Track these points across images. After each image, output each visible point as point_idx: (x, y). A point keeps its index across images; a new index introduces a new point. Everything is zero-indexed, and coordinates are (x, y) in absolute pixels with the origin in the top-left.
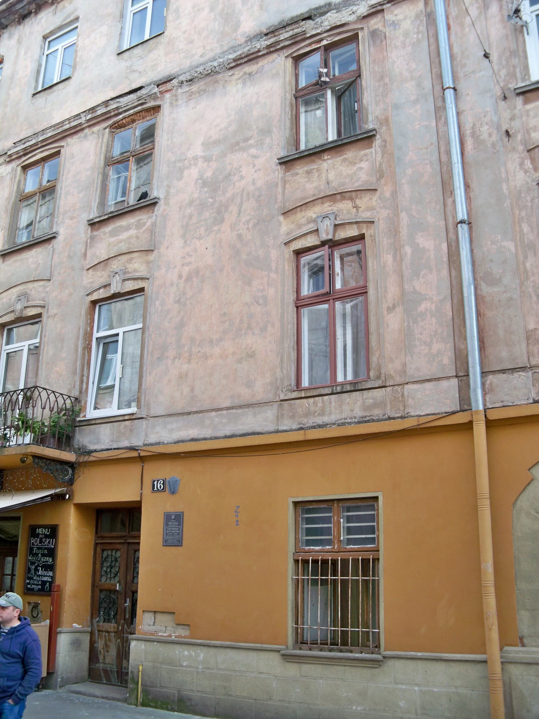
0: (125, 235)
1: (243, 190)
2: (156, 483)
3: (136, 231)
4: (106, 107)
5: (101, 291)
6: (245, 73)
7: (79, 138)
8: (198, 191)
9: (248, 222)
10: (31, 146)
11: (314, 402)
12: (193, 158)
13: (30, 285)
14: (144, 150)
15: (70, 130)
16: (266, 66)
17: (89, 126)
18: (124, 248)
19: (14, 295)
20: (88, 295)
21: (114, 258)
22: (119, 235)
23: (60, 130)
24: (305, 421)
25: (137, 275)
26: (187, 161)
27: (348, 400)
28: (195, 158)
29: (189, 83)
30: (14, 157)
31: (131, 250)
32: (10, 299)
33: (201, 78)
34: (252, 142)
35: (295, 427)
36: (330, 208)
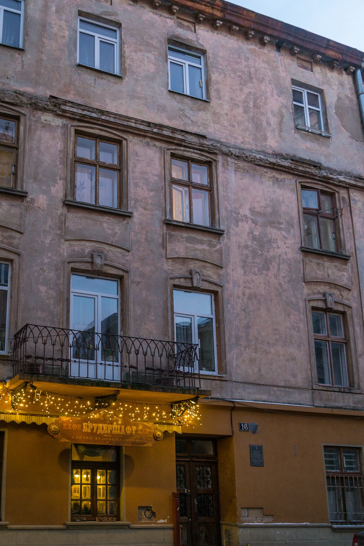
0: (199, 247)
1: (280, 255)
2: (242, 425)
3: (208, 248)
5: (182, 280)
6: (274, 177)
7: (140, 141)
8: (251, 242)
9: (284, 277)
11: (331, 394)
12: (244, 215)
13: (107, 248)
14: (202, 188)
15: (134, 130)
16: (286, 180)
17: (151, 138)
18: (200, 255)
19: (88, 248)
20: (171, 279)
21: (190, 260)
22: (195, 244)
23: (126, 123)
24: (327, 403)
25: (211, 280)
26: (240, 215)
27: (346, 397)
28: (245, 216)
29: (236, 158)
30: (68, 115)
31: (206, 260)
32: (83, 250)
33: (245, 160)
35: (322, 405)
36: (329, 290)
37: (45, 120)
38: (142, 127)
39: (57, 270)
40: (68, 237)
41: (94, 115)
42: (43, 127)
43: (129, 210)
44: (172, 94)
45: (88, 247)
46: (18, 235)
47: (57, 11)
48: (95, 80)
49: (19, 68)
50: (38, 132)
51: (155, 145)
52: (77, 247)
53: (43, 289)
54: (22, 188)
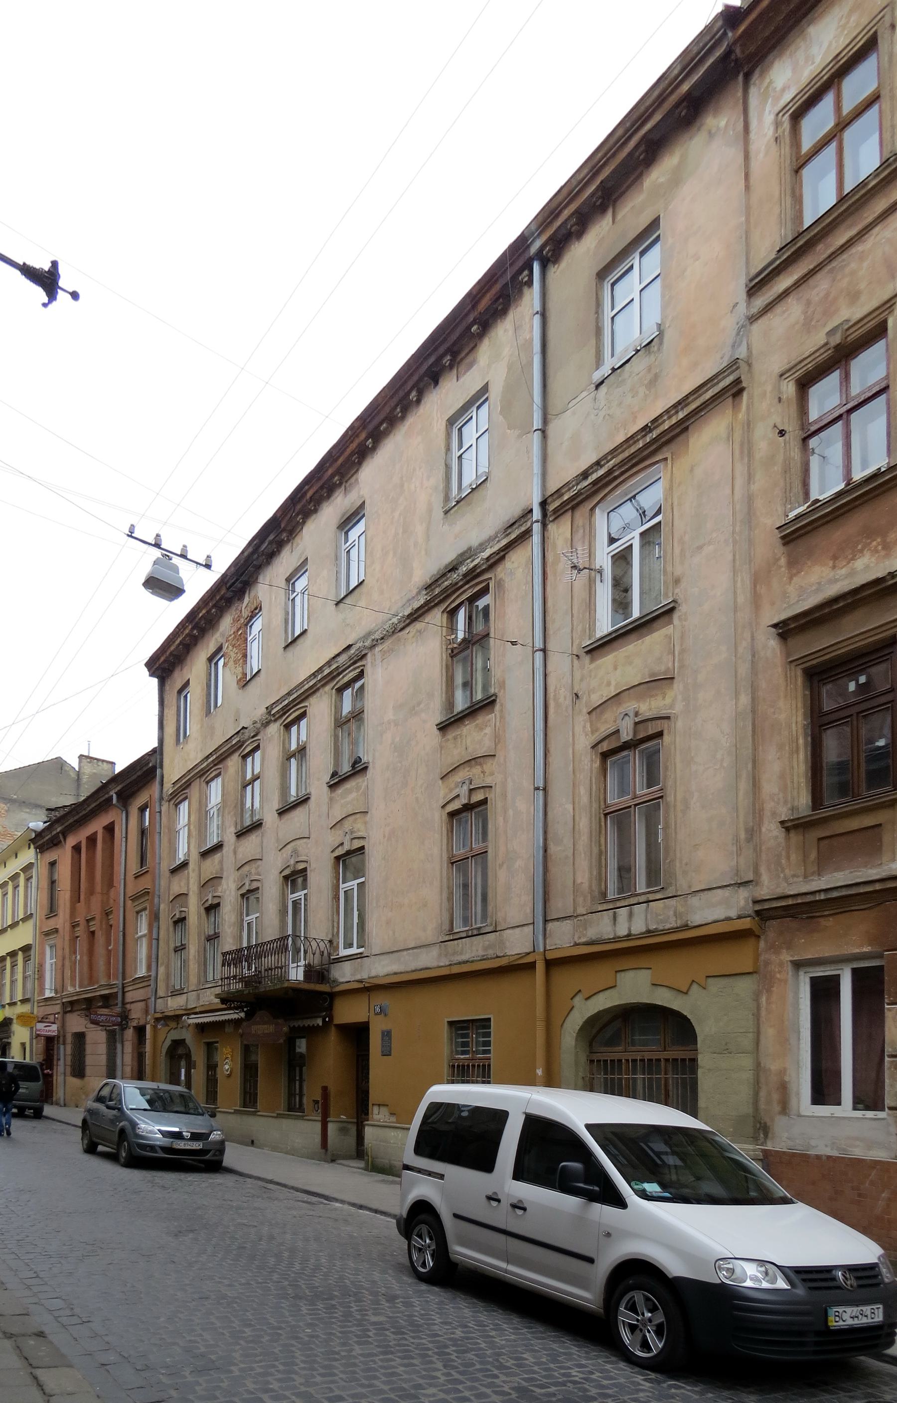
4: (330, 666)
10: (286, 706)
13: (298, 842)
27: (475, 943)
34: (422, 706)
35: (447, 963)
36: (468, 774)
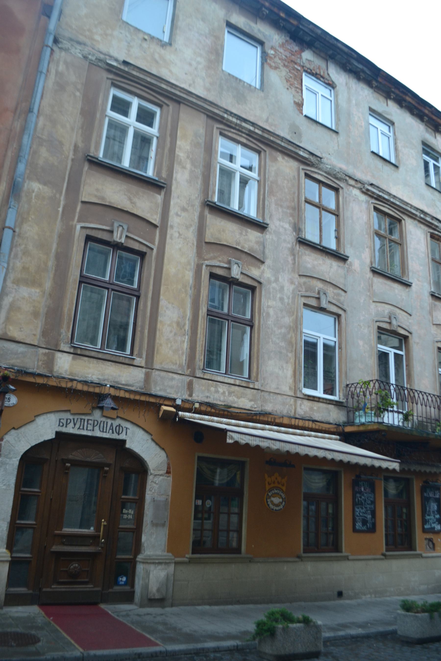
17: (419, 221)
37: (355, 195)
38: (414, 212)
39: (369, 327)
40: (375, 300)
41: (386, 197)
42: (354, 200)
43: (410, 281)
44: (427, 187)
45: (387, 309)
46: (343, 293)
47: (356, 105)
48: (382, 166)
49: (336, 148)
50: (351, 204)
51: (420, 227)
52: (381, 307)
53: (361, 343)
54: (344, 252)
